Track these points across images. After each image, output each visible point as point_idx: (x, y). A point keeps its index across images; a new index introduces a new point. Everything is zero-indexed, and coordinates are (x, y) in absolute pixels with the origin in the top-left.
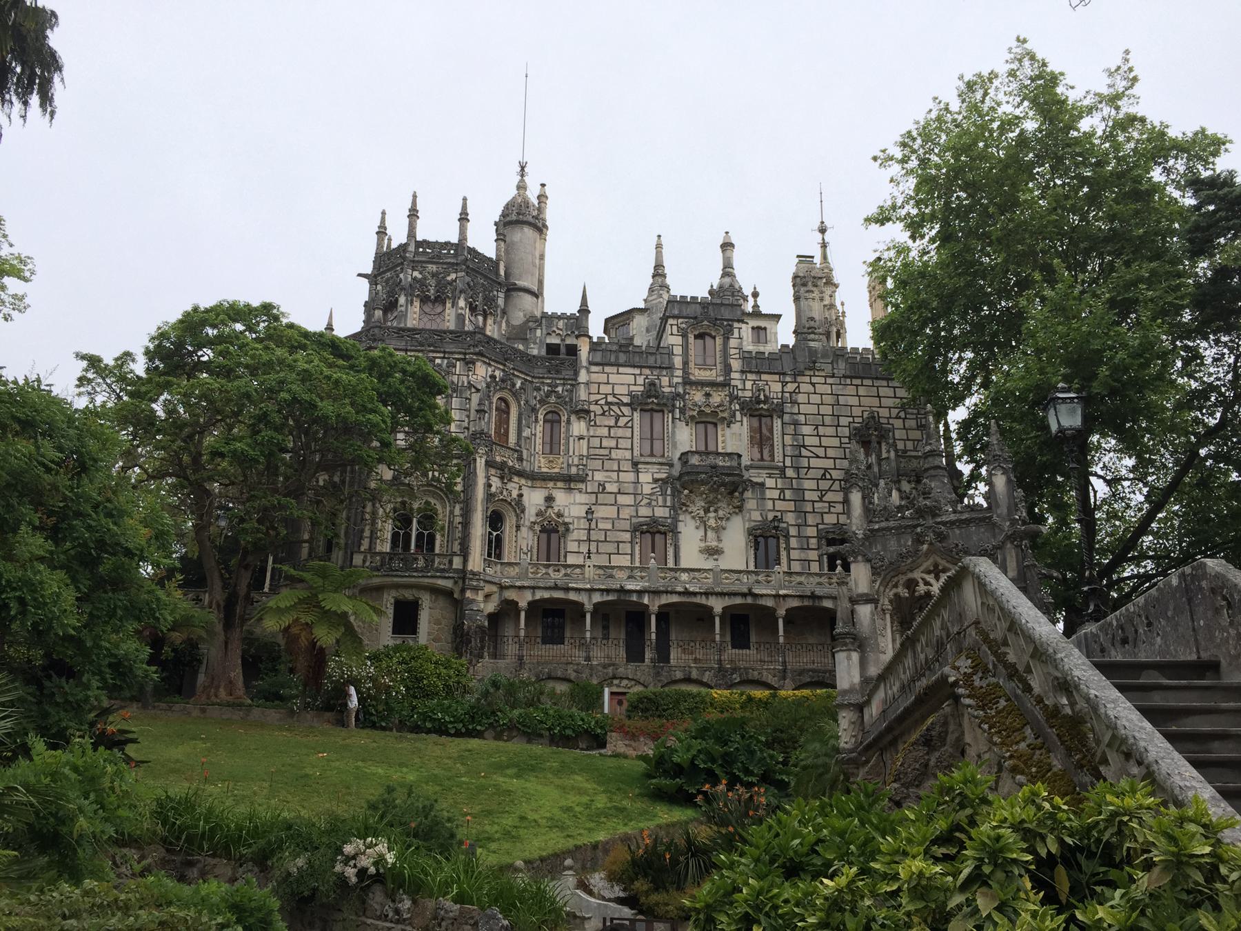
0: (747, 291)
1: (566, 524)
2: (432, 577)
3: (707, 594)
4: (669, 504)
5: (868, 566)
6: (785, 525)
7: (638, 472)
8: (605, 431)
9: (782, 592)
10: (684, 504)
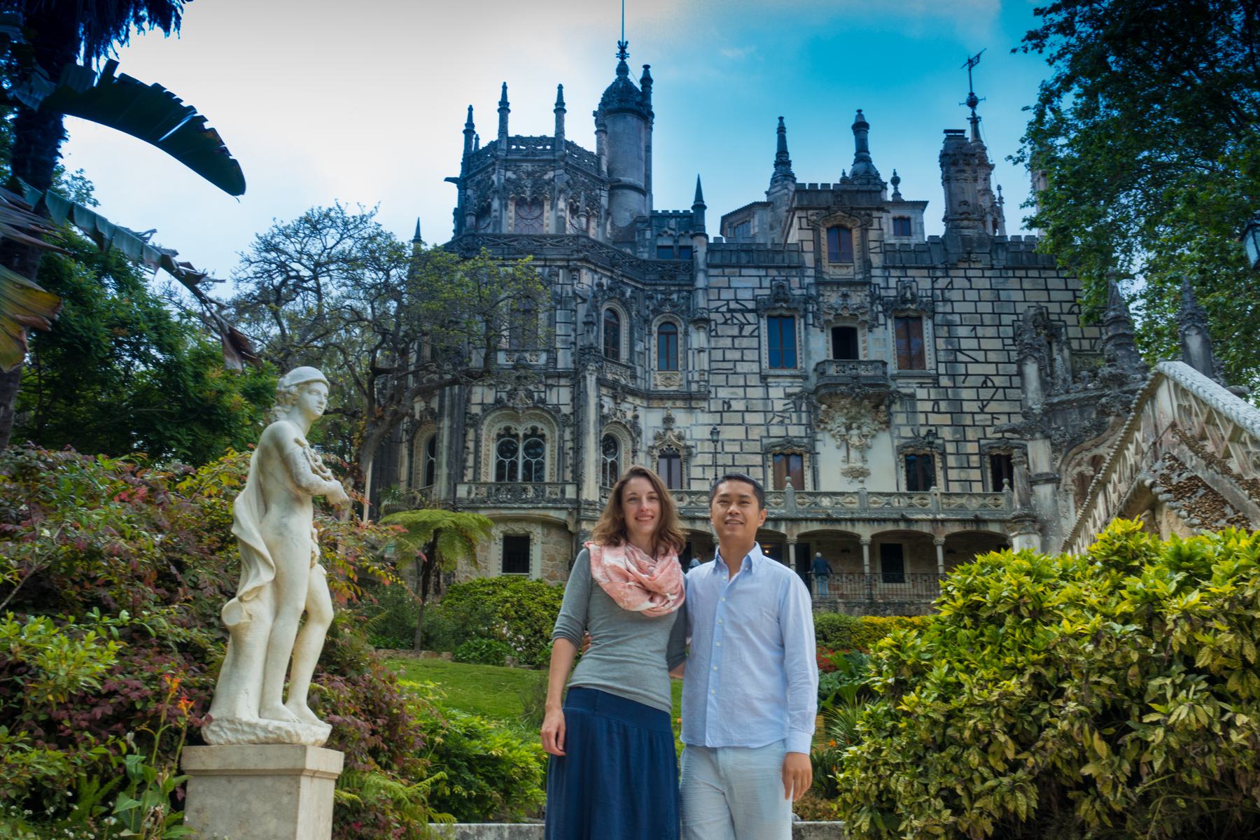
0: (886, 177)
1: (688, 448)
2: (543, 508)
3: (852, 520)
4: (804, 421)
5: (1048, 443)
6: (940, 441)
7: (767, 387)
8: (728, 342)
9: (939, 517)
10: (822, 421)
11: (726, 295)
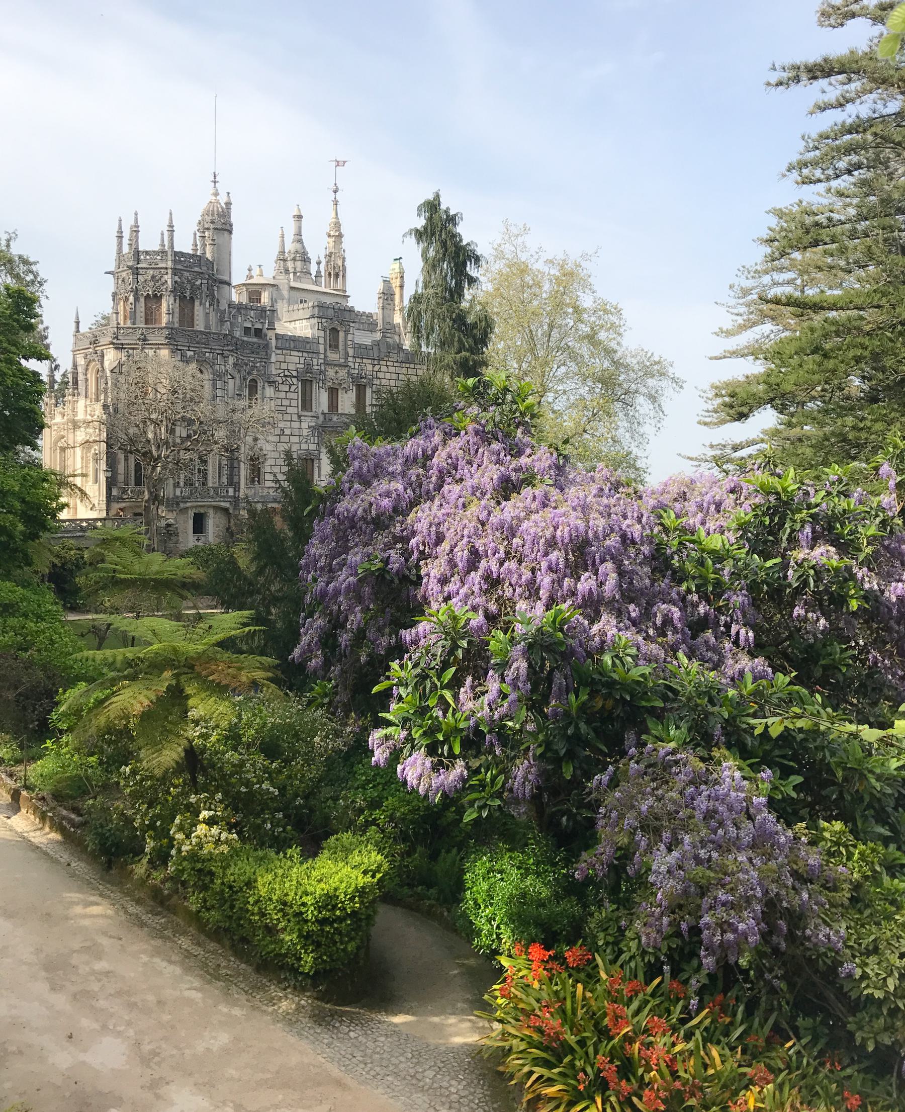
11: (284, 366)
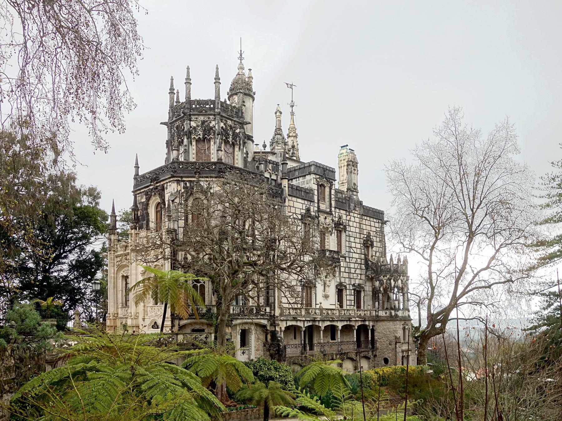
11: (293, 210)
